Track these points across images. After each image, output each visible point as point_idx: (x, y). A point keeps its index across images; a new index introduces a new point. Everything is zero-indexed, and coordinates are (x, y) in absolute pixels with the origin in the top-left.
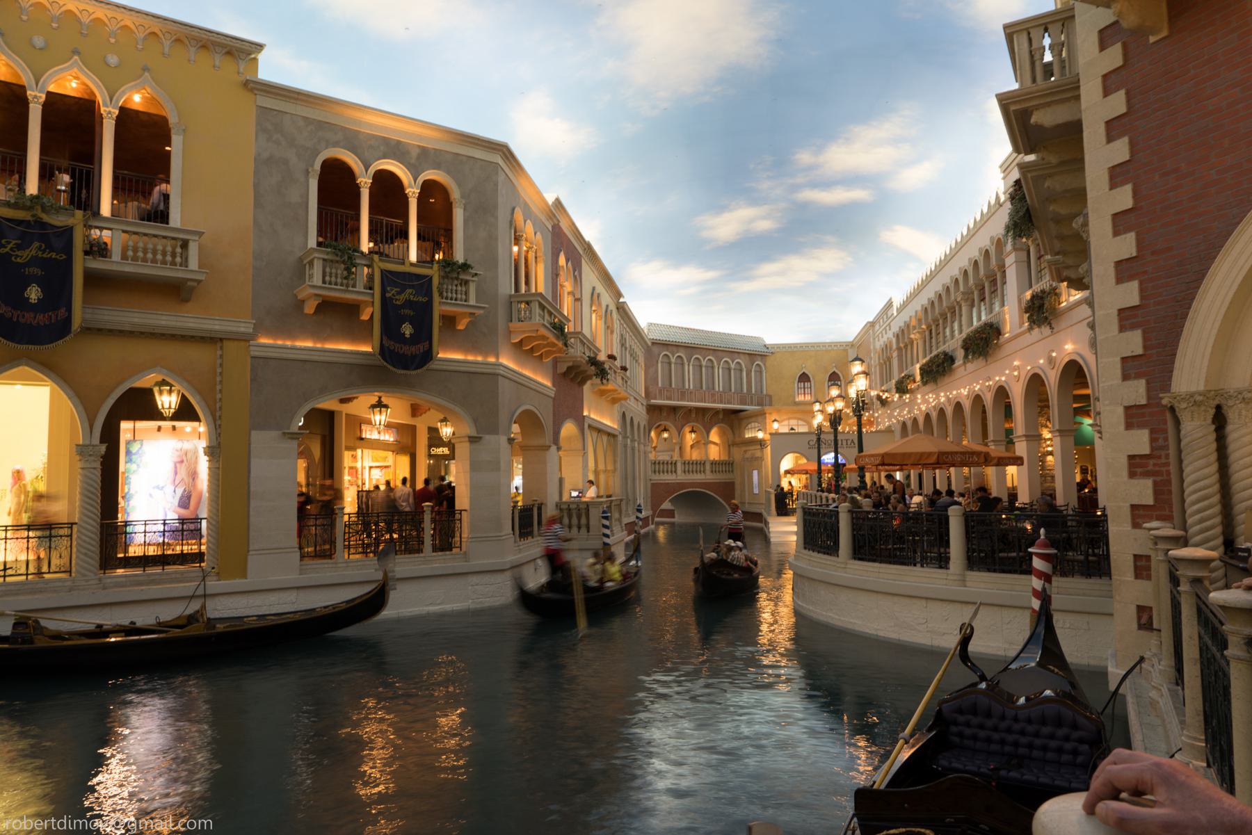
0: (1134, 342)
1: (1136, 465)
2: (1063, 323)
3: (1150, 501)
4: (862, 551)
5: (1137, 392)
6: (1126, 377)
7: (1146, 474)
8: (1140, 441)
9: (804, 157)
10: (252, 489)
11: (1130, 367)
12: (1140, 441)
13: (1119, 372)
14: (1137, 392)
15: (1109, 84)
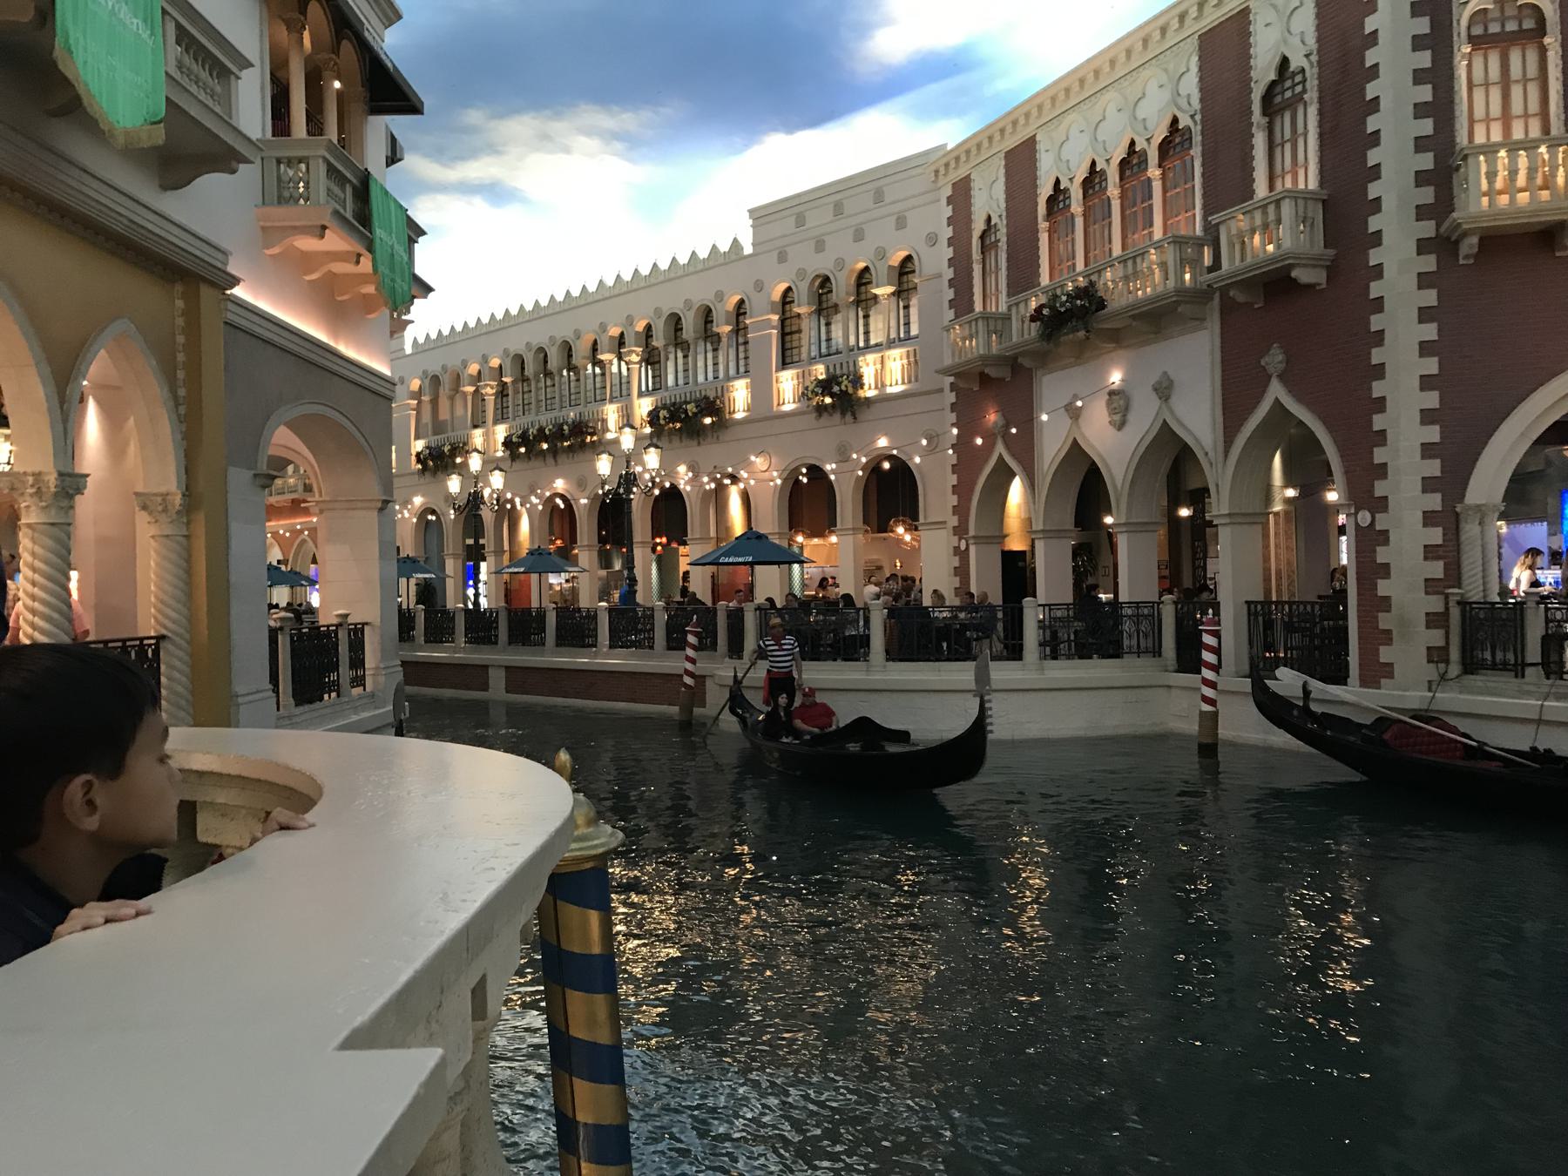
0: (1434, 468)
1: (1430, 552)
2: (865, 415)
3: (1441, 576)
4: (900, 651)
5: (1434, 501)
6: (1424, 491)
7: (1438, 558)
8: (1436, 536)
9: (474, 116)
10: (233, 579)
11: (1428, 485)
12: (1436, 536)
13: (1419, 487)
14: (1434, 501)
15: (1424, 281)
